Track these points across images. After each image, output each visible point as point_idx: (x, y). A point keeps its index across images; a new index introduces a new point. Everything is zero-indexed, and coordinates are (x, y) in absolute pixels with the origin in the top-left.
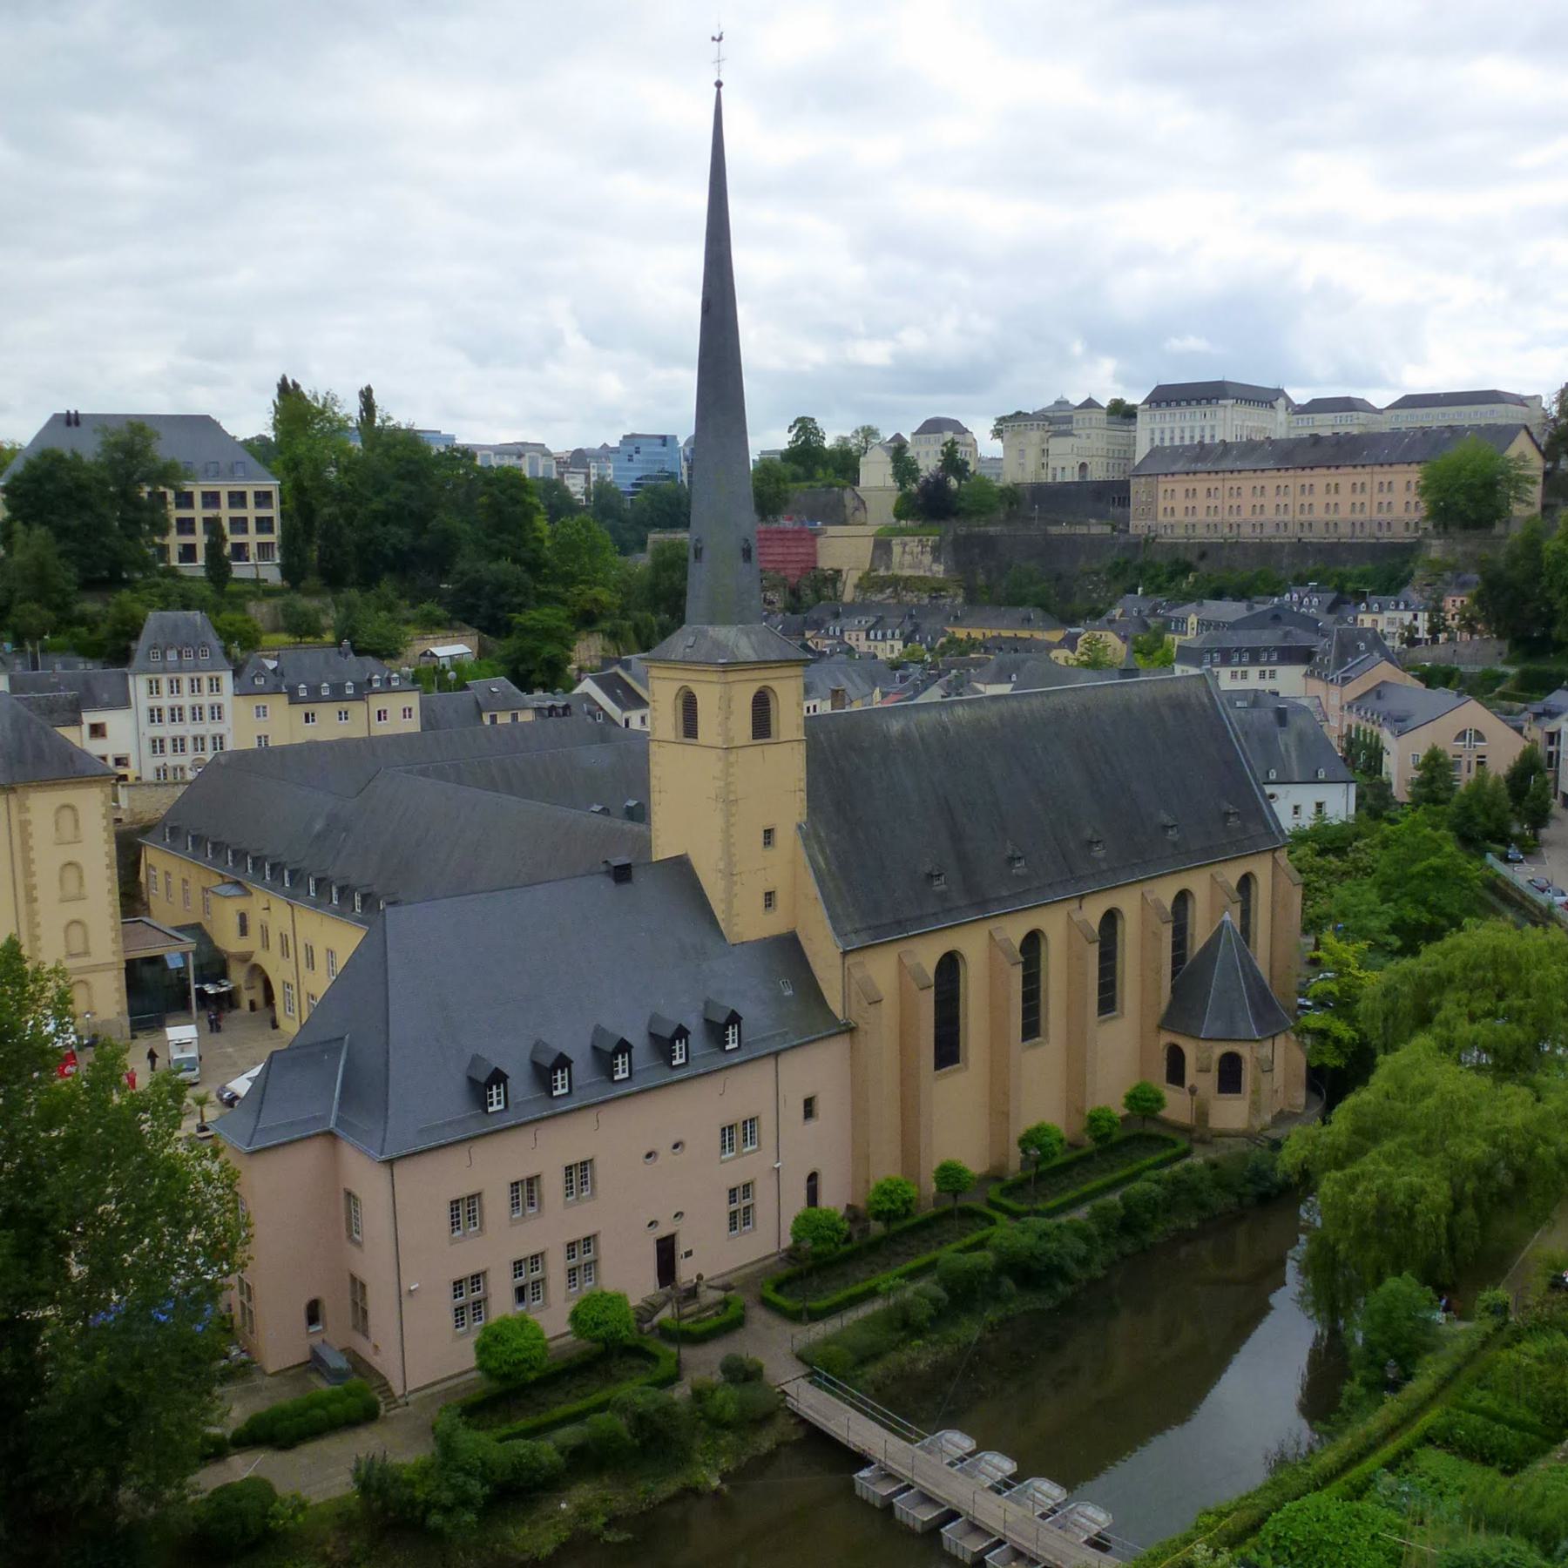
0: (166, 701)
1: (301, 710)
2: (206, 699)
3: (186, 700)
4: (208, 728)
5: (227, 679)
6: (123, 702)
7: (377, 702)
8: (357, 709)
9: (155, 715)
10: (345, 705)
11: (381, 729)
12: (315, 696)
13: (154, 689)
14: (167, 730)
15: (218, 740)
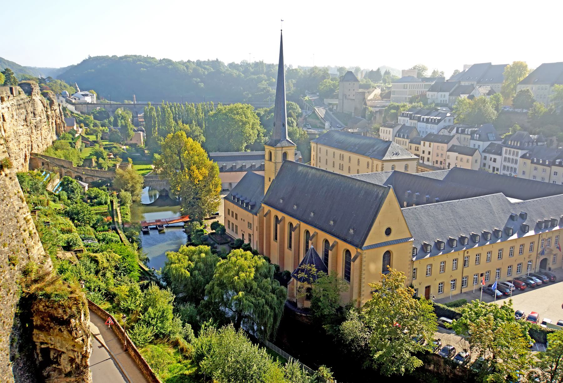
0: (508, 156)
1: (534, 165)
2: (515, 158)
3: (511, 157)
4: (513, 166)
5: (521, 153)
6: (500, 154)
7: (554, 168)
8: (548, 169)
9: (505, 160)
10: (545, 167)
11: (554, 178)
12: (538, 163)
13: (506, 153)
14: (507, 164)
15: (515, 169)
